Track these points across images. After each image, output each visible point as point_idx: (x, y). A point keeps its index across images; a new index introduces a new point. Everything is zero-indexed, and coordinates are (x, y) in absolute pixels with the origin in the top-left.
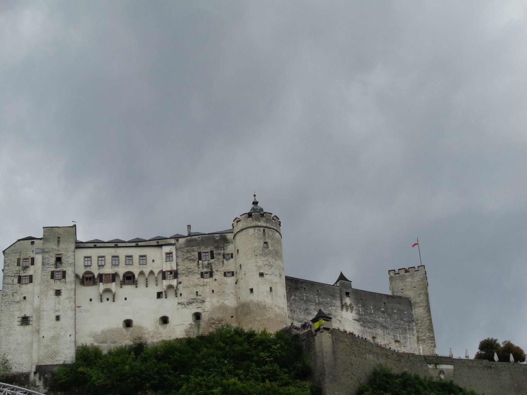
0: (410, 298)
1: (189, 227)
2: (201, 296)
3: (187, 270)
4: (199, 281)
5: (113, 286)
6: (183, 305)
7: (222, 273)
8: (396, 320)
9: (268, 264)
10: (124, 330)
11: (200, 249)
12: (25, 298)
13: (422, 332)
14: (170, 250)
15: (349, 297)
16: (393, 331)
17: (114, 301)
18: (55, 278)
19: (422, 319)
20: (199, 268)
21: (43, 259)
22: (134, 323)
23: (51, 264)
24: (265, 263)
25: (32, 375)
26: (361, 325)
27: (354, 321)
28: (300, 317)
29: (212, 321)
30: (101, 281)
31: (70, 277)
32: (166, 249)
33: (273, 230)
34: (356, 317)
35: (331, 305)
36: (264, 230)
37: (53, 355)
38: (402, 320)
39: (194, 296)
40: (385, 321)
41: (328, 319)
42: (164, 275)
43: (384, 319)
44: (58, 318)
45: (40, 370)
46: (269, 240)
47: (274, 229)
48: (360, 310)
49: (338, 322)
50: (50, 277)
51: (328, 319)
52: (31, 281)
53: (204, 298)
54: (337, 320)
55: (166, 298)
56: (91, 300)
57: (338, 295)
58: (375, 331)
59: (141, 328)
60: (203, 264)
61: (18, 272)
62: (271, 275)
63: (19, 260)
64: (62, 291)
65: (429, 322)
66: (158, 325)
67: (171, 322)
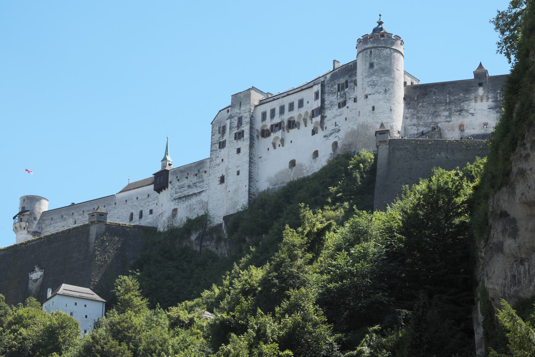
9: (372, 84)
10: (290, 170)
12: (222, 160)
20: (338, 100)
23: (235, 127)
28: (428, 121)
30: (272, 132)
31: (247, 135)
33: (380, 49)
36: (371, 52)
39: (333, 127)
42: (314, 114)
44: (238, 173)
47: (380, 47)
50: (234, 138)
54: (470, 113)
59: (301, 165)
63: (220, 127)
66: (312, 160)
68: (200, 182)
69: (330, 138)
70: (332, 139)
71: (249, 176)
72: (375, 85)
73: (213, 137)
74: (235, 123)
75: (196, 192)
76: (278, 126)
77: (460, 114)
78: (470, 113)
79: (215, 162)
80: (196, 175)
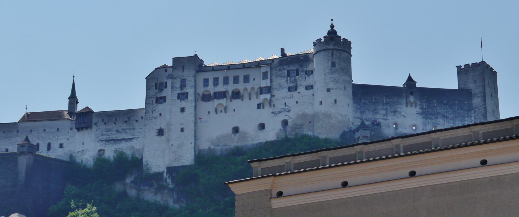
0: (471, 89)
1: (282, 50)
2: (288, 106)
3: (279, 85)
4: (287, 94)
5: (223, 101)
6: (275, 114)
7: (304, 87)
8: (456, 110)
9: (334, 80)
10: (233, 135)
11: (289, 68)
12: (160, 114)
13: (478, 119)
14: (266, 70)
15: (413, 95)
16: (453, 119)
17: (225, 112)
18: (180, 98)
19: (479, 108)
20: (287, 83)
21: (172, 84)
22: (240, 130)
23: (178, 87)
24: (332, 79)
25: (165, 174)
26: (423, 118)
27: (417, 115)
28: (369, 116)
29: (295, 126)
30: (215, 98)
31: (191, 97)
32: (263, 69)
33: (340, 51)
34: (420, 111)
35: (398, 104)
36: (332, 53)
37: (179, 159)
38: (462, 109)
39: (283, 106)
40: (446, 112)
41: (366, 129)
42: (262, 91)
43: (445, 110)
44: (182, 130)
45: (171, 170)
46: (336, 60)
47: (342, 50)
48: (424, 104)
49: (402, 117)
50: (177, 98)
51: (366, 129)
52: (165, 101)
53: (290, 108)
54: (402, 115)
55: (263, 108)
56: (209, 112)
57: (404, 95)
58: (436, 121)
60: (290, 80)
61: (156, 94)
62: (336, 89)
63: (156, 84)
64: (185, 109)
65: (484, 110)
66: (257, 130)
67: (266, 128)
68: (130, 129)
69: (278, 115)
70: (282, 117)
71: (195, 135)
72: (337, 82)
73: (148, 91)
74: (178, 84)
75: (126, 137)
76: (222, 95)
77: (394, 115)
78: (402, 115)
79: (151, 114)
80: (126, 122)
